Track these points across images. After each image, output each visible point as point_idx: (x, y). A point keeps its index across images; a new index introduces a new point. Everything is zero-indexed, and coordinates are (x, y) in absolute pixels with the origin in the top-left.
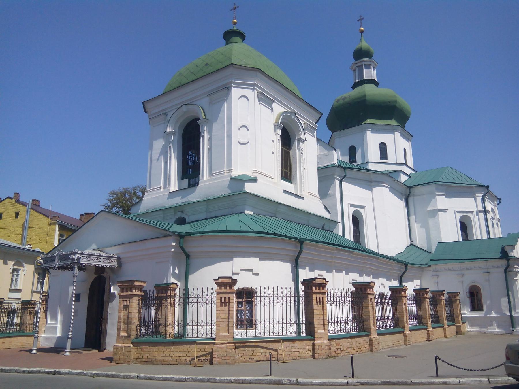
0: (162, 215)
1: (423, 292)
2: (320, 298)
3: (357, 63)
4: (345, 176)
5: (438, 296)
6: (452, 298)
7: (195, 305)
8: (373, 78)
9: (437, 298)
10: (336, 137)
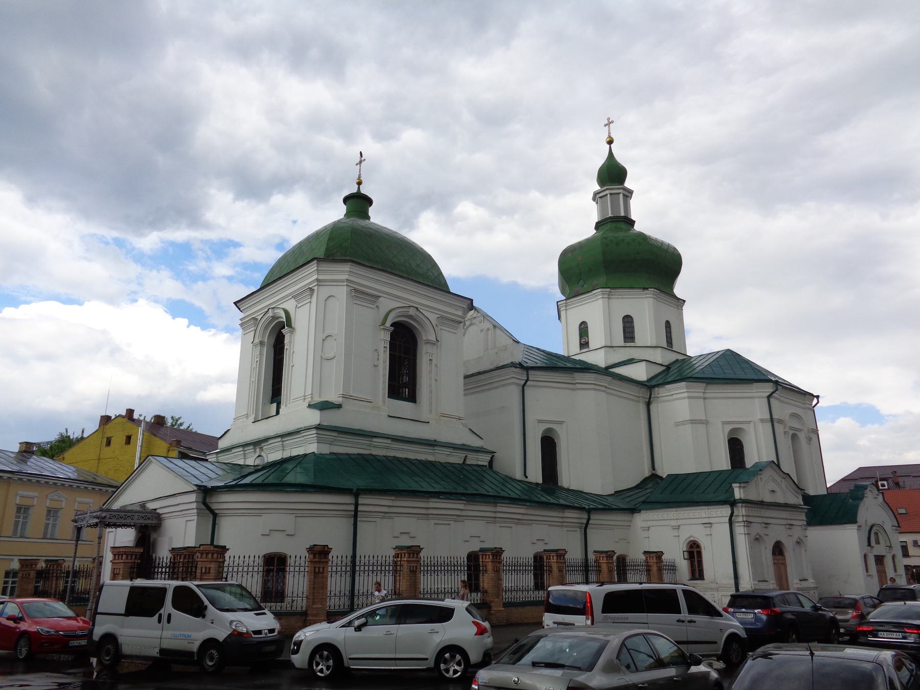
0: (242, 452)
2: (319, 568)
5: (601, 558)
8: (622, 214)
9: (600, 561)
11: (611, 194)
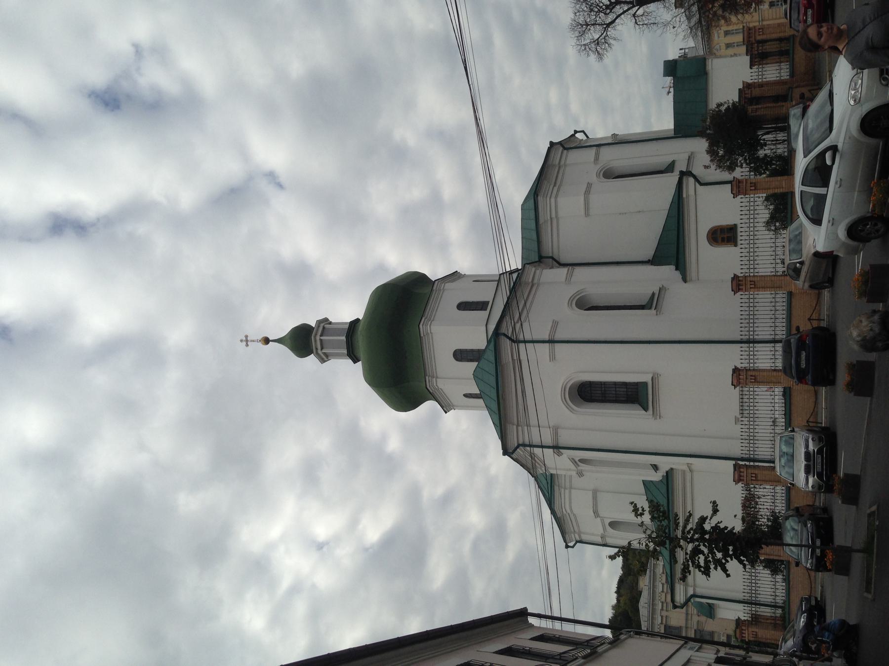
3: (317, 349)
7: (755, 453)
8: (347, 326)
10: (435, 385)
11: (320, 336)
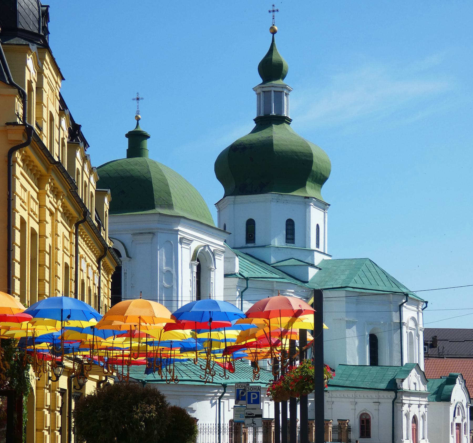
1: (311, 422)
4: (247, 288)
6: (342, 425)
